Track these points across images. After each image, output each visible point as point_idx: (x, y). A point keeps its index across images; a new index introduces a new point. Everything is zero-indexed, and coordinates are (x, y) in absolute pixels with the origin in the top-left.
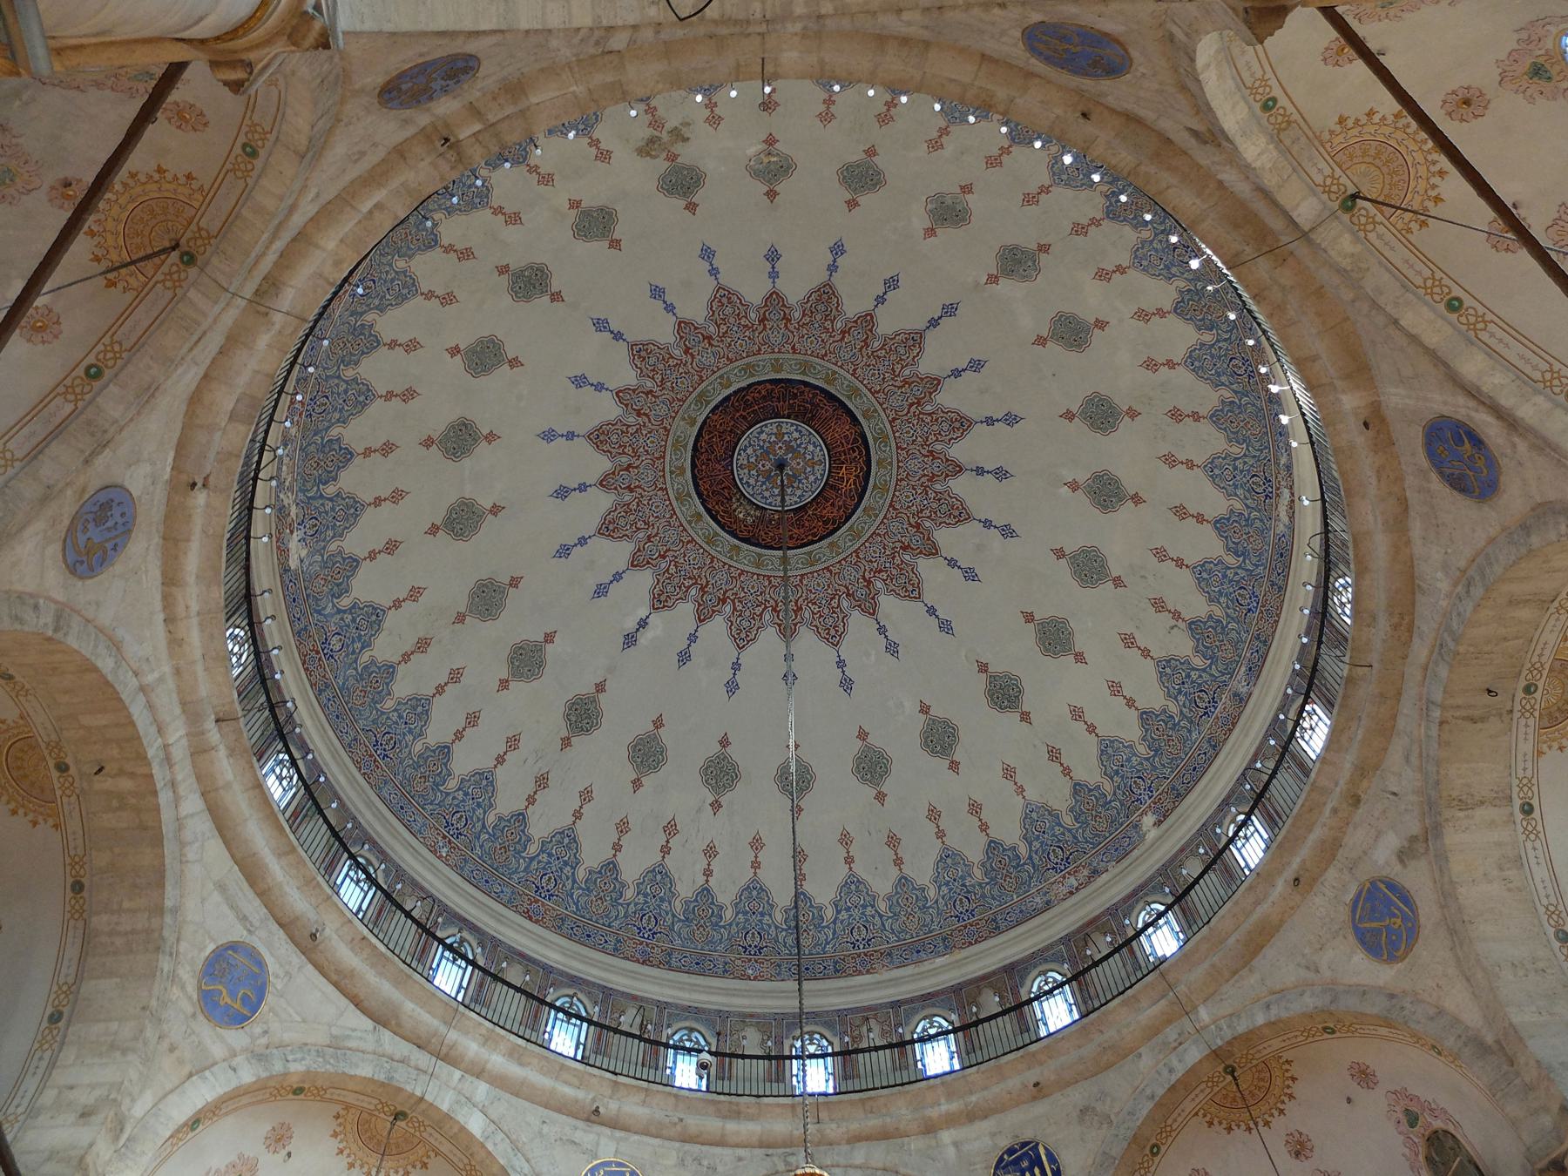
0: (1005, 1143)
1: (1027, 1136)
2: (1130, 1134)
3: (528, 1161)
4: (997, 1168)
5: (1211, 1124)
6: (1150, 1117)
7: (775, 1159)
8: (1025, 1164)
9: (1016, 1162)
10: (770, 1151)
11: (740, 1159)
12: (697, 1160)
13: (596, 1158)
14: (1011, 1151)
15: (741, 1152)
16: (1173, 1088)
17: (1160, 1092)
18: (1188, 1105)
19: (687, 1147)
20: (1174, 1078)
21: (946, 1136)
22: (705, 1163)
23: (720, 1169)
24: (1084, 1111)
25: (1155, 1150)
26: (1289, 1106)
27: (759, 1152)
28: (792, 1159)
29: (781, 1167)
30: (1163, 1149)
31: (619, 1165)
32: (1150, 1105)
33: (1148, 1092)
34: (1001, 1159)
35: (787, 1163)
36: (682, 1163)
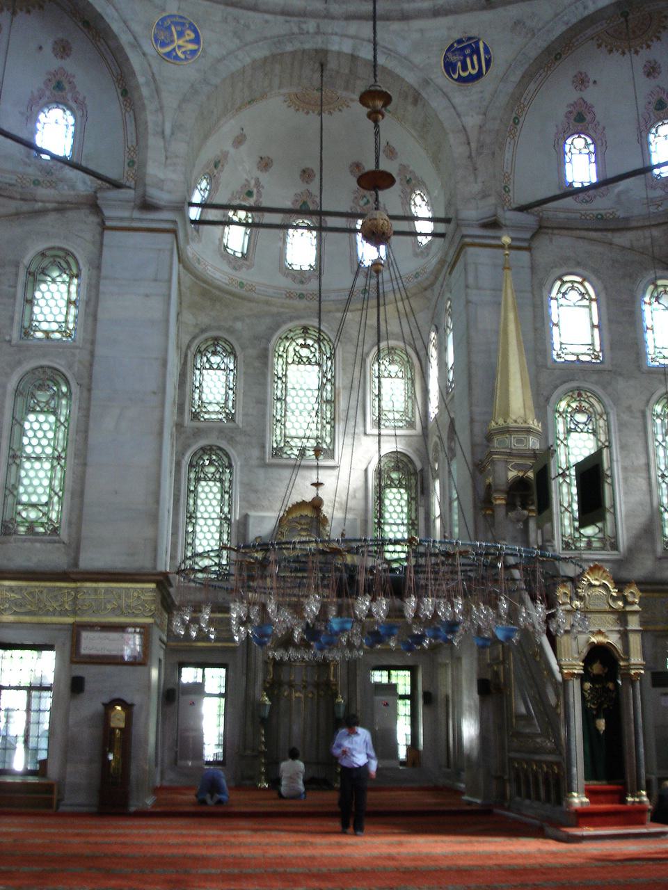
0: (457, 36)
1: (473, 33)
2: (545, 45)
3: (117, 10)
4: (448, 50)
5: (599, 46)
6: (562, 36)
7: (292, 24)
8: (468, 52)
9: (462, 49)
10: (288, 18)
11: (267, 22)
12: (237, 20)
13: (164, 10)
14: (459, 41)
15: (267, 17)
16: (583, 20)
17: (574, 20)
18: (589, 32)
19: (230, 9)
20: (586, 13)
21: (417, 24)
22: (242, 22)
23: (252, 27)
24: (518, 23)
25: (558, 57)
26: (656, 45)
27: (281, 19)
28: (304, 26)
29: (296, 30)
30: (563, 56)
31: (181, 17)
32: (564, 28)
33: (566, 18)
34: (452, 46)
35: (300, 28)
36: (225, 20)
